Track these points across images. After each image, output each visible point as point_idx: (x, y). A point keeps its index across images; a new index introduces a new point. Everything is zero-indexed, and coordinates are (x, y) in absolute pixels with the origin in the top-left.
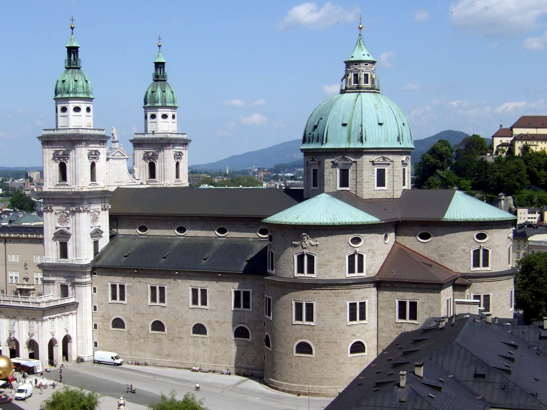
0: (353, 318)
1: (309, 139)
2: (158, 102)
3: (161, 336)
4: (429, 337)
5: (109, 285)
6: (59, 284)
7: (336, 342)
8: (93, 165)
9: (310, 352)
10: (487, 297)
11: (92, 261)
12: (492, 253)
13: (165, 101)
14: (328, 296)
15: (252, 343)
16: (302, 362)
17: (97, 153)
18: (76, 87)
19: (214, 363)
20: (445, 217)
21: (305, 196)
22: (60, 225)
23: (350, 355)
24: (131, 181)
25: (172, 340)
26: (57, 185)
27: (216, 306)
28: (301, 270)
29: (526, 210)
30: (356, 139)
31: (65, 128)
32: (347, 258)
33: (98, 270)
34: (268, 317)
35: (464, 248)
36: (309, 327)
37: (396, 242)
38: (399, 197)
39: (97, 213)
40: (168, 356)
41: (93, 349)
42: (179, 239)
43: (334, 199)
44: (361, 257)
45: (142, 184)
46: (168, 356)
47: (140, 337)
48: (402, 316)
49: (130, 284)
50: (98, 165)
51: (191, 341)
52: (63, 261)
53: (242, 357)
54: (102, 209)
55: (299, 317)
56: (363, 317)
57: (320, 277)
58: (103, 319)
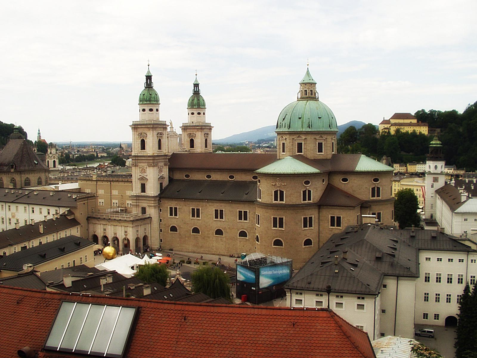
0: (305, 226)
1: (280, 126)
3: (198, 236)
4: (349, 237)
7: (296, 240)
8: (160, 141)
9: (282, 245)
10: (379, 214)
11: (159, 194)
12: (382, 189)
13: (199, 105)
14: (292, 214)
15: (249, 240)
16: (277, 251)
17: (161, 134)
18: (150, 98)
19: (228, 251)
20: (356, 169)
21: (278, 158)
23: (304, 247)
24: (180, 149)
25: (204, 238)
26: (141, 152)
27: (228, 219)
28: (276, 199)
29: (398, 165)
30: (306, 126)
32: (302, 192)
33: (162, 199)
34: (258, 226)
35: (366, 186)
36: (281, 231)
37: (329, 183)
38: (330, 158)
39: (162, 168)
40: (202, 247)
41: (160, 243)
43: (295, 159)
44: (309, 192)
45: (186, 151)
46: (202, 247)
47: (186, 237)
48: (333, 225)
50: (161, 140)
52: (143, 194)
53: (243, 248)
54: (165, 165)
55: (275, 226)
56: (311, 226)
57: (287, 203)
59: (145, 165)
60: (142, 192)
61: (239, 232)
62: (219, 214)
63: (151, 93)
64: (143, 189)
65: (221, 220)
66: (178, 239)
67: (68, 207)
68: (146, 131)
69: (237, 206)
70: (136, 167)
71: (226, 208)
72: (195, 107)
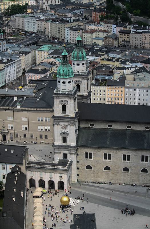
2: (81, 59)
5: (85, 153)
6: (62, 153)
15: (149, 175)
18: (69, 73)
19: (132, 182)
22: (63, 130)
26: (61, 114)
27: (134, 161)
31: (65, 90)
40: (112, 179)
42: (110, 130)
46: (112, 179)
47: (99, 173)
49: (94, 152)
51: (122, 174)
52: (64, 144)
58: (81, 166)
59: (67, 123)
60: (63, 143)
61: (142, 169)
62: (126, 158)
63: (69, 70)
64: (64, 140)
65: (128, 161)
66: (92, 174)
67: (15, 163)
68: (66, 99)
69: (141, 152)
70: (58, 125)
71: (132, 154)
72: (80, 60)
